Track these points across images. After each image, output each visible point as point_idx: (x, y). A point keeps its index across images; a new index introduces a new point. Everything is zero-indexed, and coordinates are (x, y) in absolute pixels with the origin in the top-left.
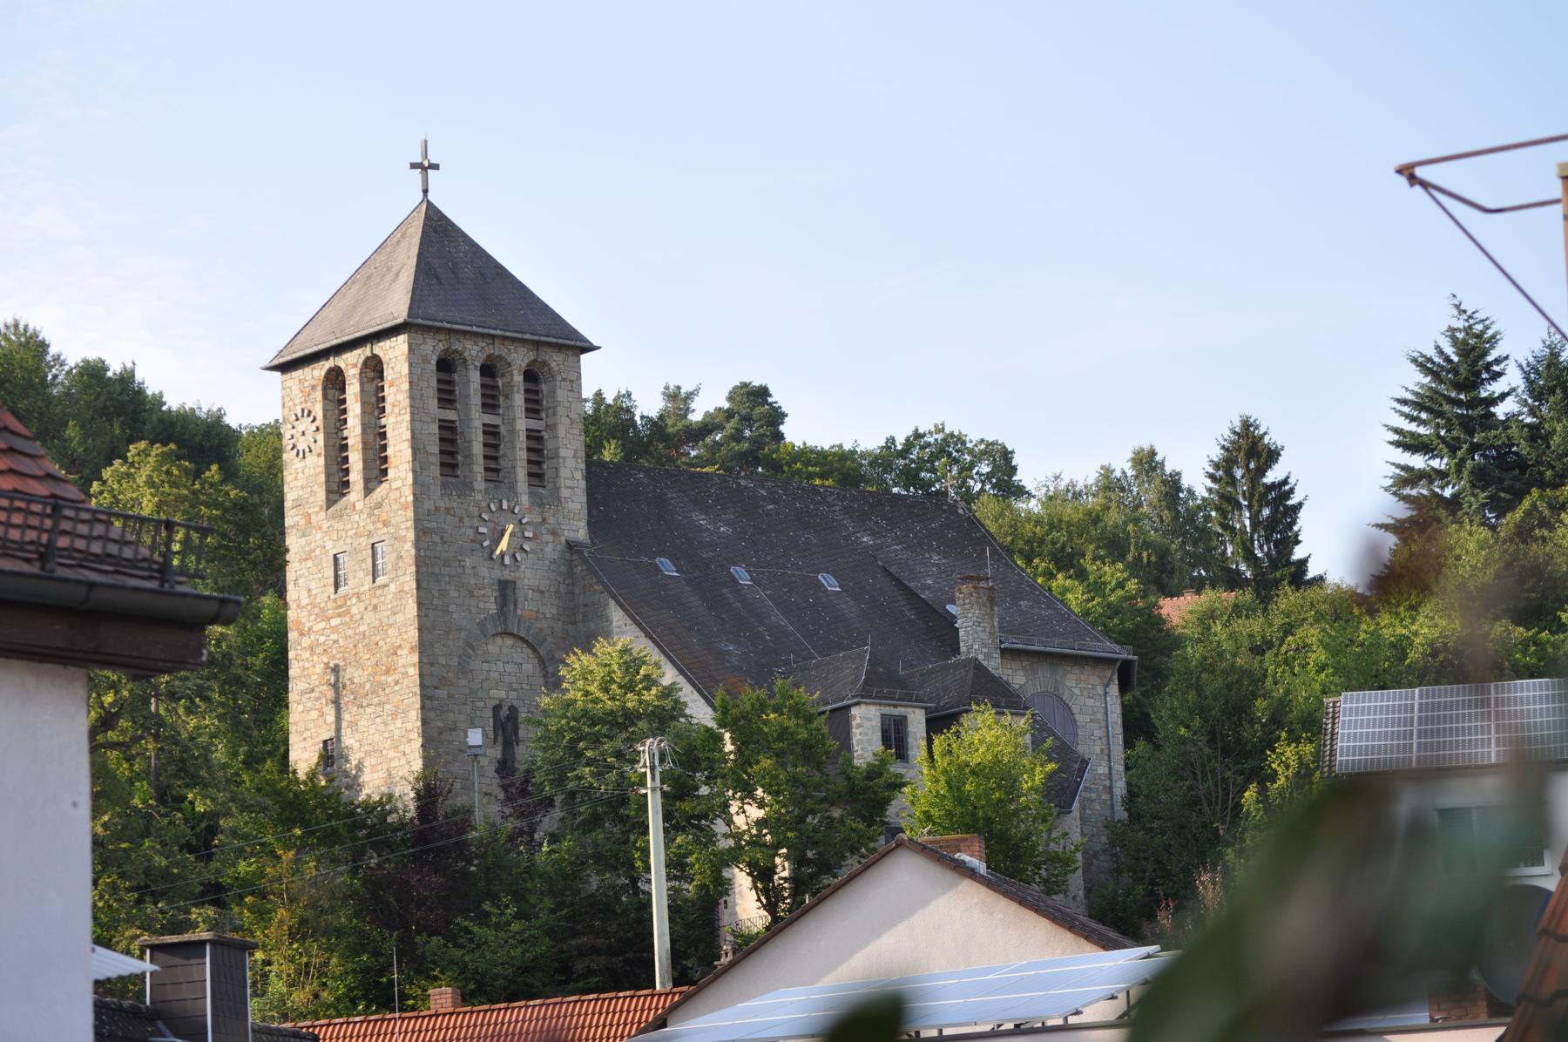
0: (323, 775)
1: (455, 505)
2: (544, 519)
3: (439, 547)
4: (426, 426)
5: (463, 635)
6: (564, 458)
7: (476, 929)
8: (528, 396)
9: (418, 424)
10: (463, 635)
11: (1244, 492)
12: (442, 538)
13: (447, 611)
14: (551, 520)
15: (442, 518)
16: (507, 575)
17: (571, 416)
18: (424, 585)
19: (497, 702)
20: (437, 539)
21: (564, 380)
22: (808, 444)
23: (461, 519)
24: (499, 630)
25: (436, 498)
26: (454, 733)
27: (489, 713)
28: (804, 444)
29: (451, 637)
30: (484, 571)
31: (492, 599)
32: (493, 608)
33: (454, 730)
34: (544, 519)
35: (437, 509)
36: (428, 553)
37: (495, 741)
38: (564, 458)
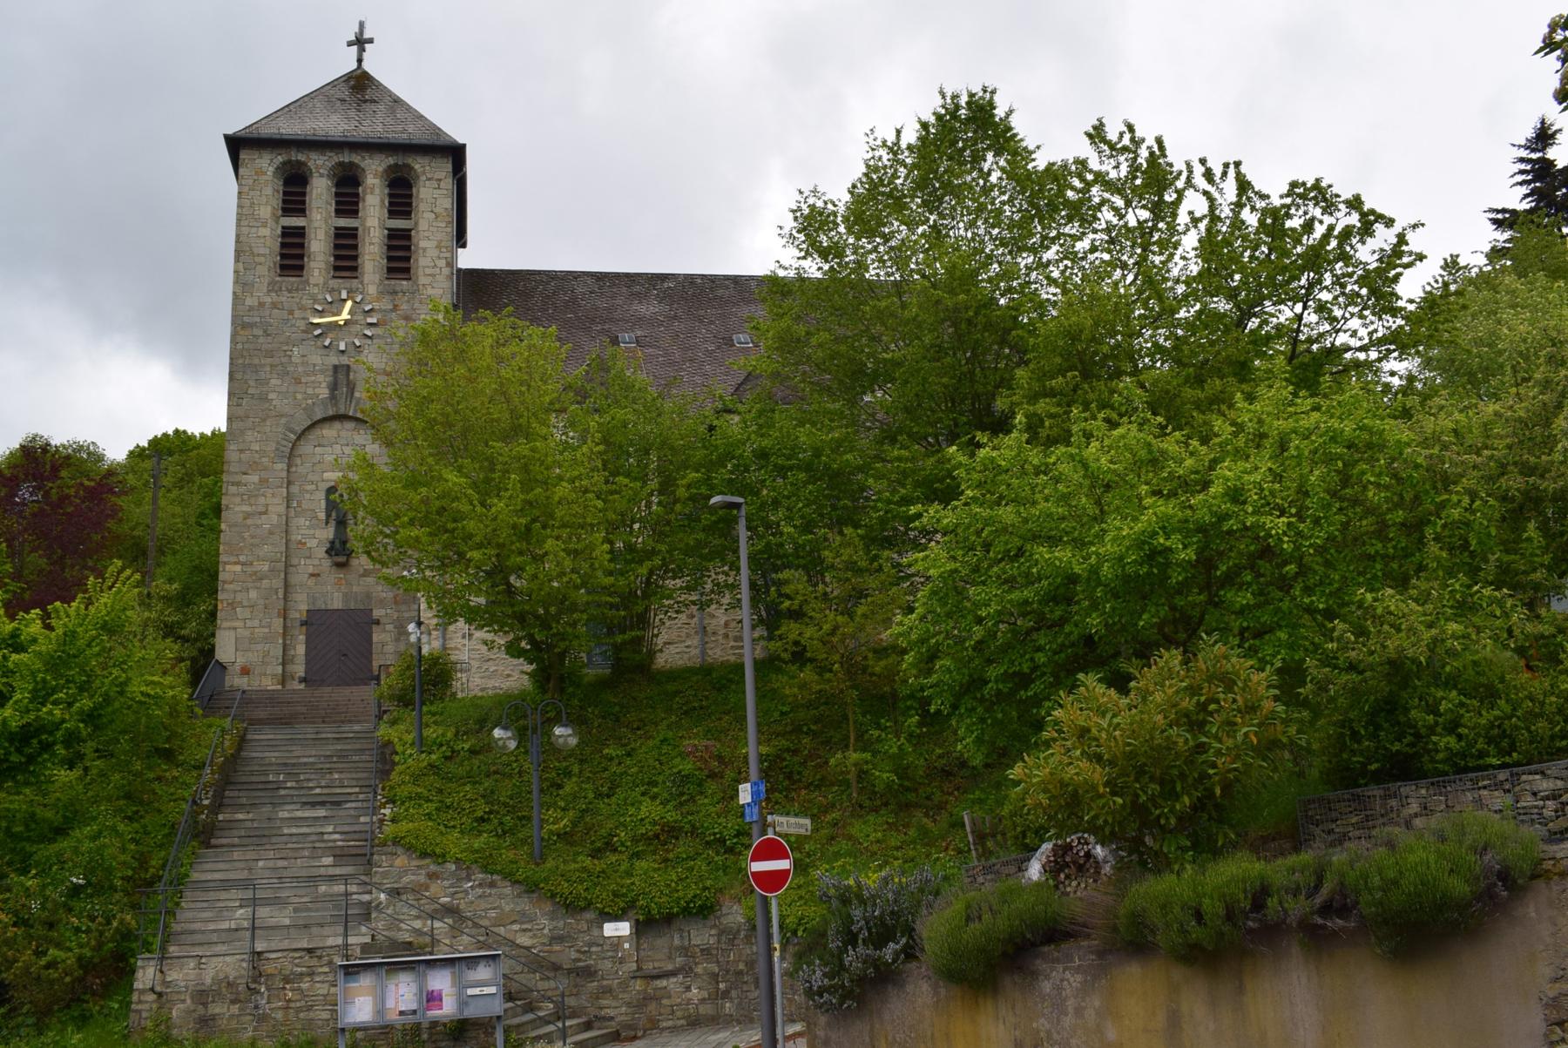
0: (1200, 312)
1: (284, 299)
2: (395, 306)
3: (261, 340)
4: (254, 230)
5: (283, 421)
6: (424, 250)
7: (413, 877)
8: (338, 253)
9: (245, 230)
10: (283, 421)
11: (1376, 331)
12: (265, 331)
13: (264, 398)
14: (404, 307)
15: (268, 313)
16: (344, 360)
17: (436, 210)
18: (238, 376)
19: (333, 484)
20: (260, 332)
21: (429, 179)
22: (1015, 121)
23: (291, 312)
24: (331, 413)
25: (260, 294)
26: (263, 517)
27: (322, 495)
28: (1010, 112)
29: (268, 423)
30: (316, 359)
31: (324, 385)
32: (324, 392)
33: (265, 513)
34: (395, 306)
35: (261, 305)
36: (246, 346)
37: (327, 523)
38: (424, 250)
